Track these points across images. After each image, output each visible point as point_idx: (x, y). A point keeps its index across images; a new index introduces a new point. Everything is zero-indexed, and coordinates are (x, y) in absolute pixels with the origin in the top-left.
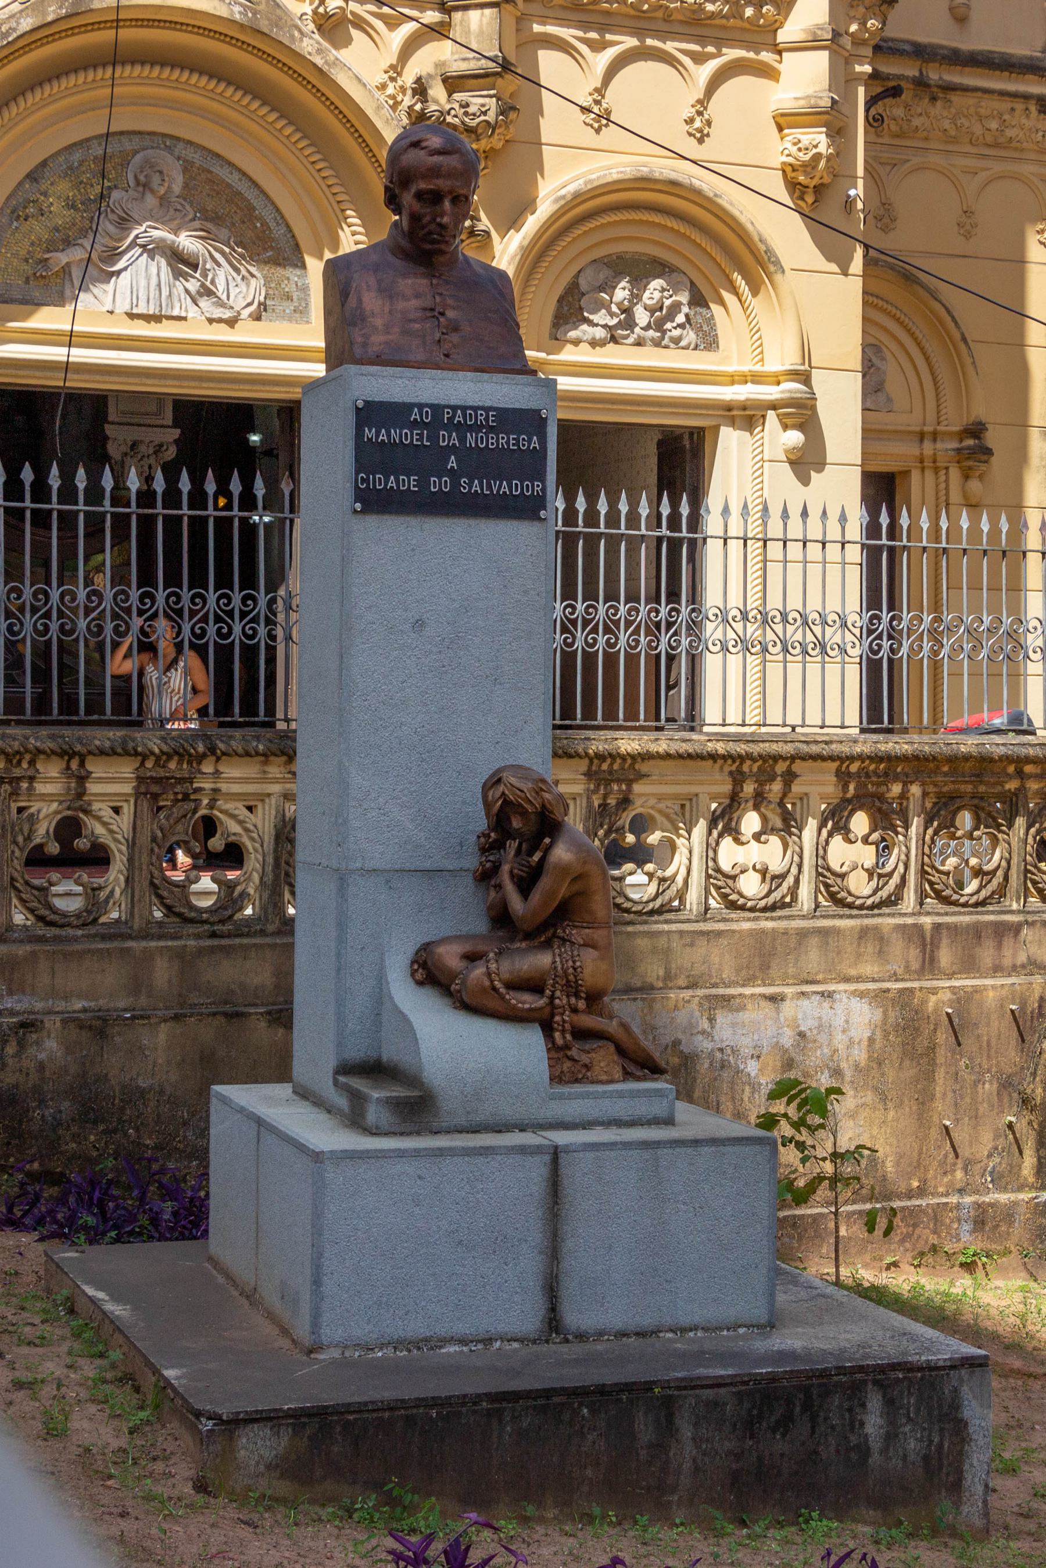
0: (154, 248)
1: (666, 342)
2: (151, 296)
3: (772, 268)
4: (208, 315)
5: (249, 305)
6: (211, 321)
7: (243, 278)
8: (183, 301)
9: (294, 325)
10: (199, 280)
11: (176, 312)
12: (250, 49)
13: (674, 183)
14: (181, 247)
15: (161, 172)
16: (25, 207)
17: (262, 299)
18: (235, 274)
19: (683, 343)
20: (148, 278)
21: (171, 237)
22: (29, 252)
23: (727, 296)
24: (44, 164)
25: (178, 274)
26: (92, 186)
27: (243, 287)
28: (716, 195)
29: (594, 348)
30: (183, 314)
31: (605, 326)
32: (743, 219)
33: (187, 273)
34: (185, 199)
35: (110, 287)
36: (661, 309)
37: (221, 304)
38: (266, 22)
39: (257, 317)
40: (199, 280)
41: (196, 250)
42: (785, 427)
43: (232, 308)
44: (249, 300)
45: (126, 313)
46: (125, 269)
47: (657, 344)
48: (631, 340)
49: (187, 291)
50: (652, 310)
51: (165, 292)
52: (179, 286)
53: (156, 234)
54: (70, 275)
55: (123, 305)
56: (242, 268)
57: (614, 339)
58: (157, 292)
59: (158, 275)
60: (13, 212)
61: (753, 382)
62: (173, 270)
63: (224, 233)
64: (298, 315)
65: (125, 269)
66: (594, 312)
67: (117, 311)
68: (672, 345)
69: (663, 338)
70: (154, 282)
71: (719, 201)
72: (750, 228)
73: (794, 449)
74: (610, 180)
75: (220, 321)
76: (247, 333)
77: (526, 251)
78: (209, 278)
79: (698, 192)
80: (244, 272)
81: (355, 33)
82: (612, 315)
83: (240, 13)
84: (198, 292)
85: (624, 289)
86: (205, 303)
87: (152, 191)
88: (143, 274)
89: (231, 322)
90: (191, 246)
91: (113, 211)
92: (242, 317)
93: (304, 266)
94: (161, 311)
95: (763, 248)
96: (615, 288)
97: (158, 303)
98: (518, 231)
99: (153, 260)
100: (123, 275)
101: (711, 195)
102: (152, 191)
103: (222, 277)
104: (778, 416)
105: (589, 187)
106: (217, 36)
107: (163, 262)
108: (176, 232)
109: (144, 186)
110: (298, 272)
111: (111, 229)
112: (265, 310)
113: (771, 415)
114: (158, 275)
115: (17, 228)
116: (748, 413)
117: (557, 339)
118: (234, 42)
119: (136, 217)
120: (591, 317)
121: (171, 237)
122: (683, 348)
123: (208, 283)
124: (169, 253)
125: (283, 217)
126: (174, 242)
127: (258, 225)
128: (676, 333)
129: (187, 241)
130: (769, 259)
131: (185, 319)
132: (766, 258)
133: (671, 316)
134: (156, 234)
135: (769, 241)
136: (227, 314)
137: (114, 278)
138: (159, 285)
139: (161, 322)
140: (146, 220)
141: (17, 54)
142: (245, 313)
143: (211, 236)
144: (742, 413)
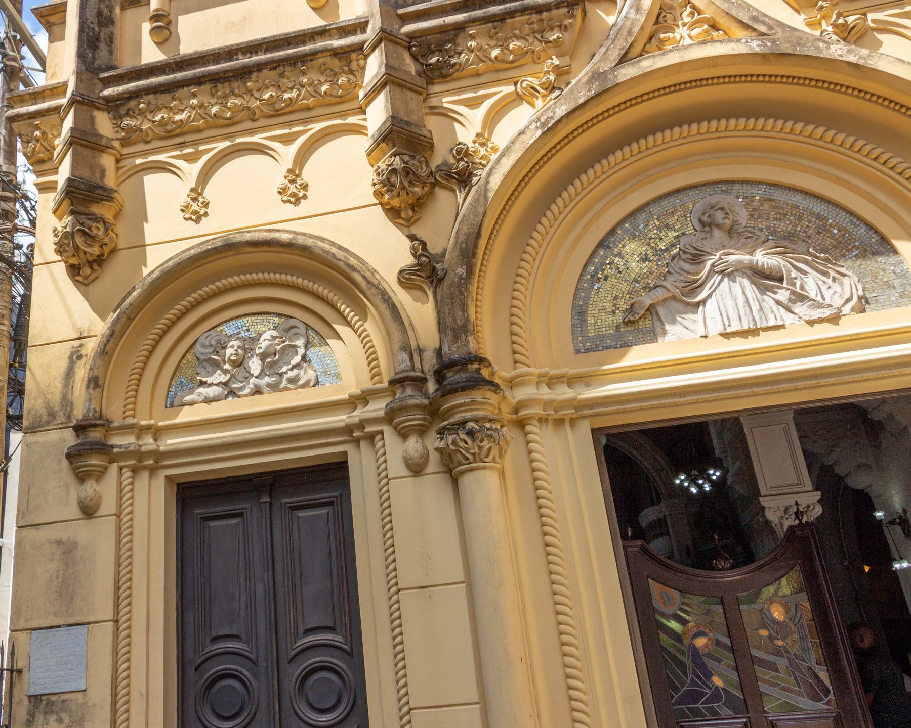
0: (732, 272)
2: (742, 314)
4: (806, 318)
5: (848, 301)
6: (811, 323)
7: (834, 279)
8: (776, 312)
9: (904, 308)
10: (788, 289)
11: (772, 323)
12: (779, 79)
14: (760, 264)
15: (722, 209)
16: (603, 270)
17: (861, 293)
18: (824, 278)
20: (735, 300)
21: (747, 257)
22: (614, 305)
24: (612, 231)
25: (764, 290)
26: (661, 239)
27: (836, 287)
30: (780, 323)
33: (773, 286)
34: (754, 228)
35: (699, 316)
37: (820, 306)
38: (788, 45)
39: (861, 309)
40: (788, 289)
41: (776, 263)
43: (831, 306)
44: (847, 296)
45: (721, 334)
46: (710, 296)
49: (778, 303)
51: (755, 308)
52: (768, 301)
53: (732, 258)
54: (658, 315)
55: (715, 327)
56: (830, 271)
58: (747, 308)
59: (744, 293)
60: (593, 276)
62: (758, 287)
63: (801, 246)
64: (906, 300)
65: (710, 296)
67: (710, 335)
70: (741, 300)
75: (821, 321)
76: (853, 325)
78: (798, 285)
80: (832, 274)
81: (880, 37)
83: (758, 45)
84: (790, 300)
86: (799, 308)
87: (719, 226)
88: (728, 296)
89: (834, 319)
90: (769, 260)
91: (685, 252)
92: (844, 313)
93: (896, 252)
94: (756, 324)
97: (751, 319)
99: (735, 281)
100: (709, 303)
102: (719, 226)
103: (811, 283)
106: (743, 79)
107: (746, 282)
108: (751, 253)
109: (710, 225)
110: (892, 259)
111: (687, 267)
112: (868, 303)
114: (744, 293)
115: (599, 288)
118: (761, 78)
119: (709, 251)
121: (746, 258)
123: (798, 290)
124: (749, 273)
125: (859, 218)
126: (751, 262)
127: (835, 231)
129: (762, 258)
131: (783, 326)
134: (732, 258)
136: (827, 313)
137: (701, 308)
138: (747, 301)
139: (758, 335)
140: (717, 250)
141: (563, 143)
142: (846, 309)
143: (789, 250)
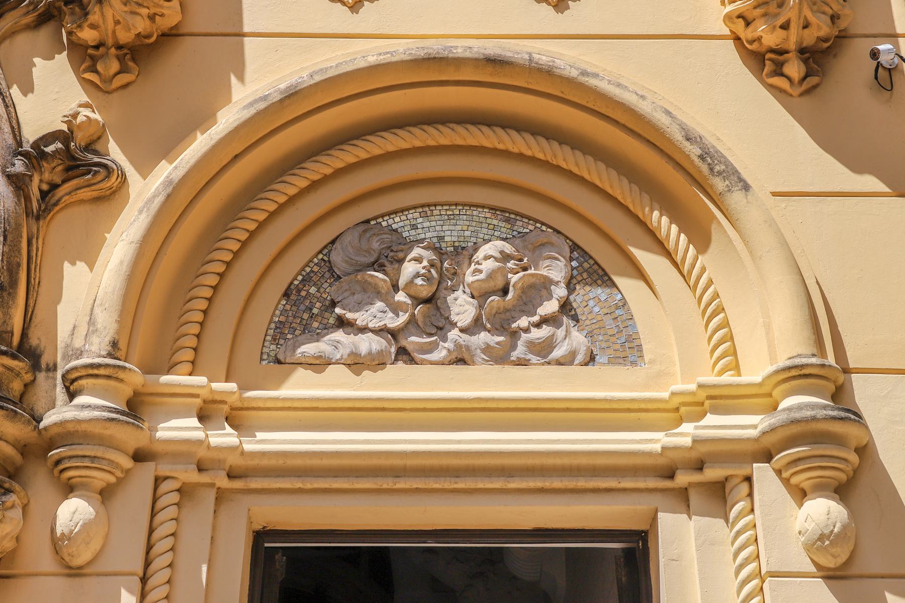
1: (520, 351)
3: (720, 184)
13: (494, 62)
19: (558, 352)
23: (647, 259)
28: (584, 73)
29: (358, 374)
31: (378, 332)
32: (644, 107)
36: (505, 291)
42: (801, 495)
47: (500, 357)
48: (440, 354)
50: (480, 296)
57: (403, 354)
61: (716, 411)
66: (359, 306)
68: (534, 359)
69: (514, 347)
71: (592, 82)
72: (662, 120)
73: (822, 537)
74: (362, 64)
77: (174, 190)
79: (548, 73)
82: (396, 309)
85: (418, 260)
95: (694, 151)
96: (401, 261)
98: (171, 163)
101: (574, 73)
104: (779, 472)
105: (317, 78)
113: (762, 472)
116: (712, 473)
117: (279, 362)
120: (350, 316)
122: (559, 363)
128: (545, 332)
130: (711, 170)
132: (705, 168)
133: (527, 303)
135: (710, 140)
144: (696, 477)
